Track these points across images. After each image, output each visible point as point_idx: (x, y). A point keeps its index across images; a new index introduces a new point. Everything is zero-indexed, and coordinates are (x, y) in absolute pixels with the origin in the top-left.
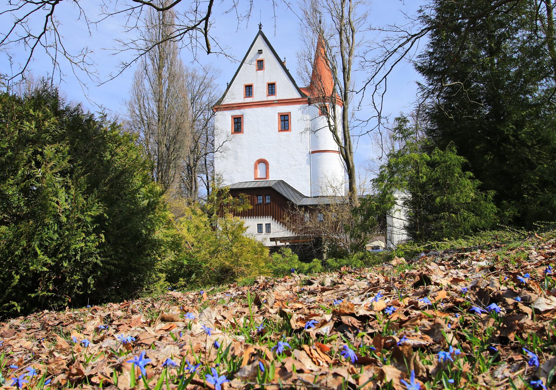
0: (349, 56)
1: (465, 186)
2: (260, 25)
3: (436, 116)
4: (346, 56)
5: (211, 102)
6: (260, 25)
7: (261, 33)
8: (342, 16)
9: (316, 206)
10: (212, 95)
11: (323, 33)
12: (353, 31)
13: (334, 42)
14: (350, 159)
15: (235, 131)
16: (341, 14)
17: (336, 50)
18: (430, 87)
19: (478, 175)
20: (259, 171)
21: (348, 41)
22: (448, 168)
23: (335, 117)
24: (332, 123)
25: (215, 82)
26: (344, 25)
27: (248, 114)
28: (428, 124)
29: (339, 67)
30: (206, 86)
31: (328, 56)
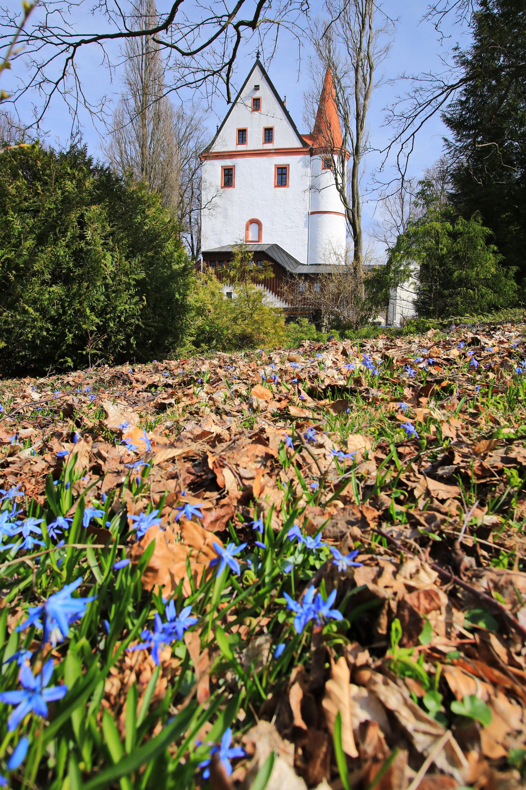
0: (365, 100)
1: (486, 261)
3: (461, 177)
4: (362, 100)
5: (199, 149)
8: (360, 48)
9: (318, 274)
10: (200, 140)
12: (371, 68)
13: (348, 81)
16: (358, 46)
17: (350, 91)
18: (458, 144)
19: (502, 250)
20: (250, 234)
21: (364, 80)
22: (470, 239)
23: (343, 175)
24: (340, 181)
25: (205, 124)
27: (241, 165)
28: (450, 188)
30: (193, 128)
31: (340, 98)
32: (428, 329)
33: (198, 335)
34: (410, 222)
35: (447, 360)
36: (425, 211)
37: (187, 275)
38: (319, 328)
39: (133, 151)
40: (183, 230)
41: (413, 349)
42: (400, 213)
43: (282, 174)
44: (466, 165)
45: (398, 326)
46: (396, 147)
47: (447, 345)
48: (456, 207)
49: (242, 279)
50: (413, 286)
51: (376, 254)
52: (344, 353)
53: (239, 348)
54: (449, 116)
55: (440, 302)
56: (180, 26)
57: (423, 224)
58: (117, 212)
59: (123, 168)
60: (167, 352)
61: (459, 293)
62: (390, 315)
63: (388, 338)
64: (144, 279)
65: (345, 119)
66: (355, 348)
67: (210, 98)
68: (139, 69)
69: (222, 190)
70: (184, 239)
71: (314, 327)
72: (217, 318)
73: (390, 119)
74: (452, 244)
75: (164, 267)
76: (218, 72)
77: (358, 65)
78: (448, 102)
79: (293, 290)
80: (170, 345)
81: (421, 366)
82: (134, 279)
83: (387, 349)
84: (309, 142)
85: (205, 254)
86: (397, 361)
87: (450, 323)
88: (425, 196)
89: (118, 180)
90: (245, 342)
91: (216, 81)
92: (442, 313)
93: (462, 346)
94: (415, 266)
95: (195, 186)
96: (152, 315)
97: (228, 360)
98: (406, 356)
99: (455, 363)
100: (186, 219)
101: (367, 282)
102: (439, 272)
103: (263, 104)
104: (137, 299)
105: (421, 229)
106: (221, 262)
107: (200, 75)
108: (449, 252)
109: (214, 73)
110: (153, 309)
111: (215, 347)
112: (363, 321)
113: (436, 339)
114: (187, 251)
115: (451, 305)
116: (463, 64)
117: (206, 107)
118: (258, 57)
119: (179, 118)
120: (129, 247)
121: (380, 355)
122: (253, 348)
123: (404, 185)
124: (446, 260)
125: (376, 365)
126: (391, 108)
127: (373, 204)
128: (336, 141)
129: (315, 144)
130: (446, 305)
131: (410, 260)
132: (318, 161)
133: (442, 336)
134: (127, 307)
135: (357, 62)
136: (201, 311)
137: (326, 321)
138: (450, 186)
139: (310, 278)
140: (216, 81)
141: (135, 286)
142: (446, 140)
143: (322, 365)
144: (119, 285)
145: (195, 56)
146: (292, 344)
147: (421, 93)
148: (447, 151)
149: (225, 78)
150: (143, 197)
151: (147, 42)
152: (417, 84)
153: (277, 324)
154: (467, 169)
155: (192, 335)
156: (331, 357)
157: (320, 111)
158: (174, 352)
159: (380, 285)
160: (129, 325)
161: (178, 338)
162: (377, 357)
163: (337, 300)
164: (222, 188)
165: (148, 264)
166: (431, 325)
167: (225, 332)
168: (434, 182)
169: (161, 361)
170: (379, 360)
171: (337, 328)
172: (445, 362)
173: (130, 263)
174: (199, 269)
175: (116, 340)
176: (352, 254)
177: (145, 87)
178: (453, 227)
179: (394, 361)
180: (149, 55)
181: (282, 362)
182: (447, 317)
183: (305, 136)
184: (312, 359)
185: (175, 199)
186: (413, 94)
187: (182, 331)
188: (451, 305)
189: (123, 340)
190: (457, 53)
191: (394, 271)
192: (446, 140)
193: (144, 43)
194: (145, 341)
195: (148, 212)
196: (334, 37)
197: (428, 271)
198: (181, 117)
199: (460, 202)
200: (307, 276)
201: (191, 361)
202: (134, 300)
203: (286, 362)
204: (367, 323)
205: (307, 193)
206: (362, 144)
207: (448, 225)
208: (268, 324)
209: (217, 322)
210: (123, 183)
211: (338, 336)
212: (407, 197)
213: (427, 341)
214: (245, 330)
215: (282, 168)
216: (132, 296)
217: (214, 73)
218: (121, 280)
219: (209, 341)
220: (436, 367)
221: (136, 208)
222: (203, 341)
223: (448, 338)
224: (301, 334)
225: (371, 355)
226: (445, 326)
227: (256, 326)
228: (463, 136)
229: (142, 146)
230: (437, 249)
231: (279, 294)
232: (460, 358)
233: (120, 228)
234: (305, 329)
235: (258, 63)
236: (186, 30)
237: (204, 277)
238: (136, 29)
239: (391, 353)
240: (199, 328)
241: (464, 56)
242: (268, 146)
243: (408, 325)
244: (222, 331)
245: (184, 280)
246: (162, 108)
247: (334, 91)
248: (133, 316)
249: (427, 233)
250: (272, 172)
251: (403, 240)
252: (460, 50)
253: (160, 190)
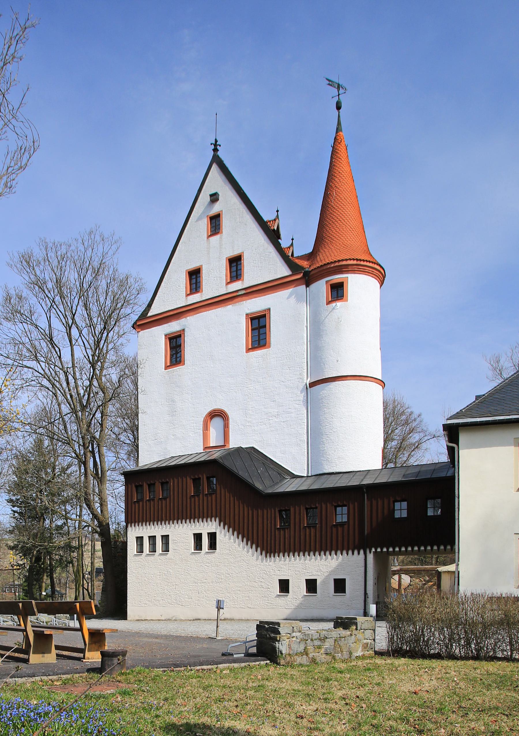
2: (215, 145)
6: (215, 145)
7: (217, 160)
103: (225, 223)
250: (242, 326)
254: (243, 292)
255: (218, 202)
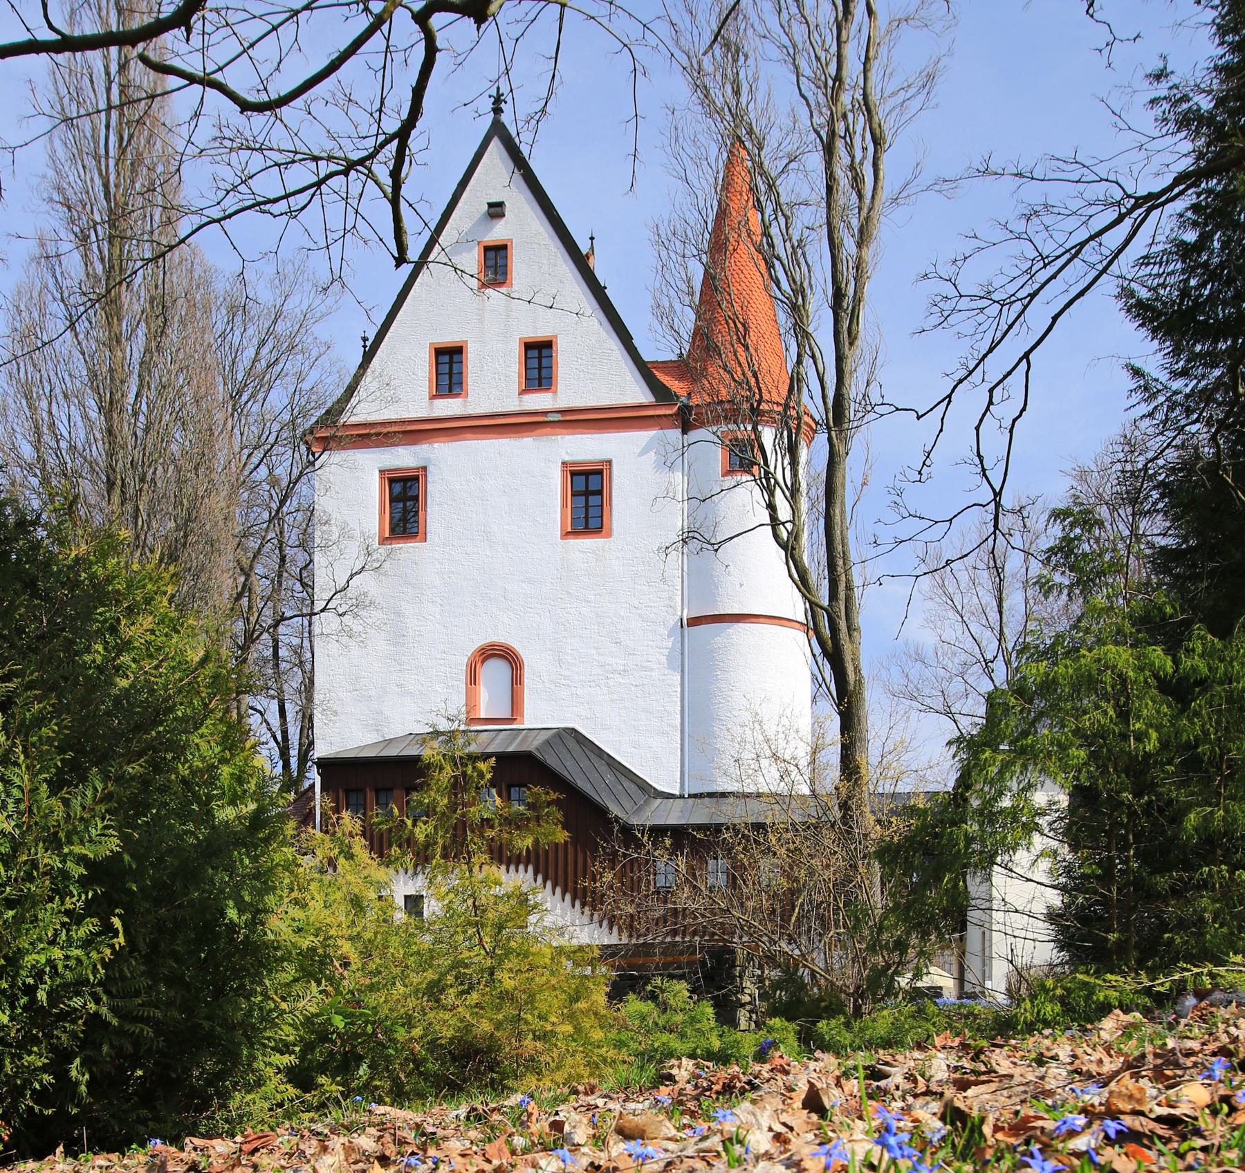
0: (860, 245)
4: (849, 246)
5: (304, 413)
8: (838, 78)
10: (306, 386)
11: (760, 149)
12: (877, 141)
13: (802, 184)
14: (848, 658)
15: (392, 530)
17: (810, 217)
18: (1177, 384)
21: (857, 181)
23: (794, 492)
24: (784, 513)
25: (321, 331)
26: (845, 116)
27: (449, 467)
28: (1158, 531)
29: (818, 290)
30: (283, 345)
31: (778, 241)
32: (1105, 1009)
33: (308, 1047)
34: (1025, 648)
35: (1170, 1121)
36: (1076, 609)
37: (267, 841)
38: (726, 1013)
39: (77, 423)
40: (249, 690)
41: (1051, 1084)
42: (993, 615)
43: (587, 493)
44: (1208, 452)
45: (1002, 999)
46: (970, 400)
47: (1168, 1070)
48: (1182, 591)
49: (456, 850)
50: (1045, 864)
51: (917, 753)
52: (814, 1103)
53: (451, 1088)
54: (1144, 294)
55: (1144, 915)
56: (233, 17)
57: (1072, 652)
58: (20, 631)
59: (45, 481)
60: (200, 1109)
61: (1205, 885)
62: (973, 962)
63: (964, 1047)
64: (116, 857)
65: (797, 310)
66: (853, 1085)
67: (336, 249)
68: (97, 157)
69: (384, 550)
70: (255, 720)
71: (710, 1011)
72: (372, 988)
73: (948, 306)
74: (1175, 717)
75: (183, 814)
76: (361, 162)
77: (832, 134)
78: (1138, 248)
79: (635, 886)
80: (209, 1083)
81: (1080, 1143)
82: (81, 860)
83: (962, 1086)
84: (676, 386)
85: (329, 767)
86: (997, 1129)
87: (1180, 989)
88: (1075, 556)
89: (23, 525)
90: (469, 1067)
91: (355, 190)
92: (1151, 952)
93: (1219, 1072)
94: (1050, 795)
95: (292, 537)
96: (145, 982)
97: (410, 1136)
98: (1026, 1111)
99: (1198, 1133)
100: (263, 647)
101: (888, 854)
102: (1132, 815)
104: (90, 926)
105: (1065, 670)
106: (383, 793)
107: (301, 175)
108: (1164, 745)
109: (351, 166)
110: (147, 959)
111: (368, 1090)
112: (878, 985)
113: (1132, 1048)
114: (266, 760)
115: (1182, 925)
116: (1184, 122)
117: (325, 277)
118: (497, 111)
119: (233, 311)
120: (61, 750)
121: (936, 1106)
122: (500, 1088)
123: (1004, 522)
124: (1154, 772)
125: (925, 1144)
126: (947, 271)
127: (900, 589)
128: (765, 381)
129: (698, 393)
130: (1163, 926)
131: (1033, 775)
132: (707, 446)
133: (1152, 1038)
134: (57, 954)
135: (831, 123)
136: (314, 966)
137: (750, 989)
138: (1160, 523)
139: (693, 841)
140: (355, 190)
141: (84, 882)
142: (1137, 372)
143: (737, 1150)
144: (29, 878)
145: (285, 111)
146: (634, 1074)
147: (1048, 220)
148: (1144, 409)
149: (387, 181)
150: (110, 579)
151: (123, 67)
152: (1033, 193)
153: (582, 1005)
154: (1213, 468)
155: (284, 1048)
156: (766, 1118)
157: (709, 279)
158: (224, 1106)
159: (934, 860)
160: (63, 1016)
161: (235, 1057)
162: (928, 1114)
163: (786, 917)
164: (383, 541)
165: (126, 807)
166: (1114, 994)
167: (401, 1034)
168: (1104, 512)
169: (176, 1140)
170: (935, 1127)
171: (788, 1011)
172: (1161, 1130)
173: (66, 803)
174: (307, 818)
175: (20, 1069)
176: (833, 756)
177: (116, 216)
178: (1176, 662)
179: (987, 1130)
180: (131, 112)
181: (599, 1140)
182: (1167, 967)
183: (664, 366)
184: (702, 1126)
185: (225, 582)
186: (1019, 227)
187: (251, 1035)
188: (1182, 925)
189: (44, 1069)
190: (1162, 90)
191: (980, 812)
192: (1137, 372)
193: (114, 68)
194: (121, 1070)
195: (128, 631)
196: (750, 43)
197: (1096, 812)
198: (239, 309)
199: (1196, 578)
200: (679, 834)
201: (283, 1139)
202: (82, 932)
203: (613, 1139)
204: (891, 991)
205: (674, 555)
206: (854, 390)
207: (1157, 654)
208: (551, 1002)
209: (372, 999)
210: (41, 533)
211: (792, 1039)
212: (1014, 563)
213: (1100, 1053)
214: (468, 1028)
215: (587, 474)
216: (75, 918)
217: (351, 166)
218: (34, 864)
219: (344, 1065)
220: (1132, 1147)
221: (87, 616)
222: (323, 1069)
223: (1171, 1043)
224: (665, 1037)
225: (907, 1110)
226: (1160, 1000)
227: (509, 1010)
228: (1193, 357)
229: (109, 408)
230: (1124, 737)
231: (586, 898)
232: (1215, 1113)
233: (30, 686)
234: (679, 1018)
235: (498, 130)
236: (252, 30)
237: (325, 848)
238: (89, 27)
239: (975, 1099)
240: (309, 1020)
241: (1185, 98)
242: (539, 401)
243: (1033, 997)
244: (389, 1031)
245: (255, 859)
246: (177, 281)
247: (755, 218)
248: (77, 986)
249: (1087, 683)
250: (555, 485)
251: (1007, 709)
252: (1174, 80)
253: (172, 556)
254: (557, 417)
255: (503, 221)
